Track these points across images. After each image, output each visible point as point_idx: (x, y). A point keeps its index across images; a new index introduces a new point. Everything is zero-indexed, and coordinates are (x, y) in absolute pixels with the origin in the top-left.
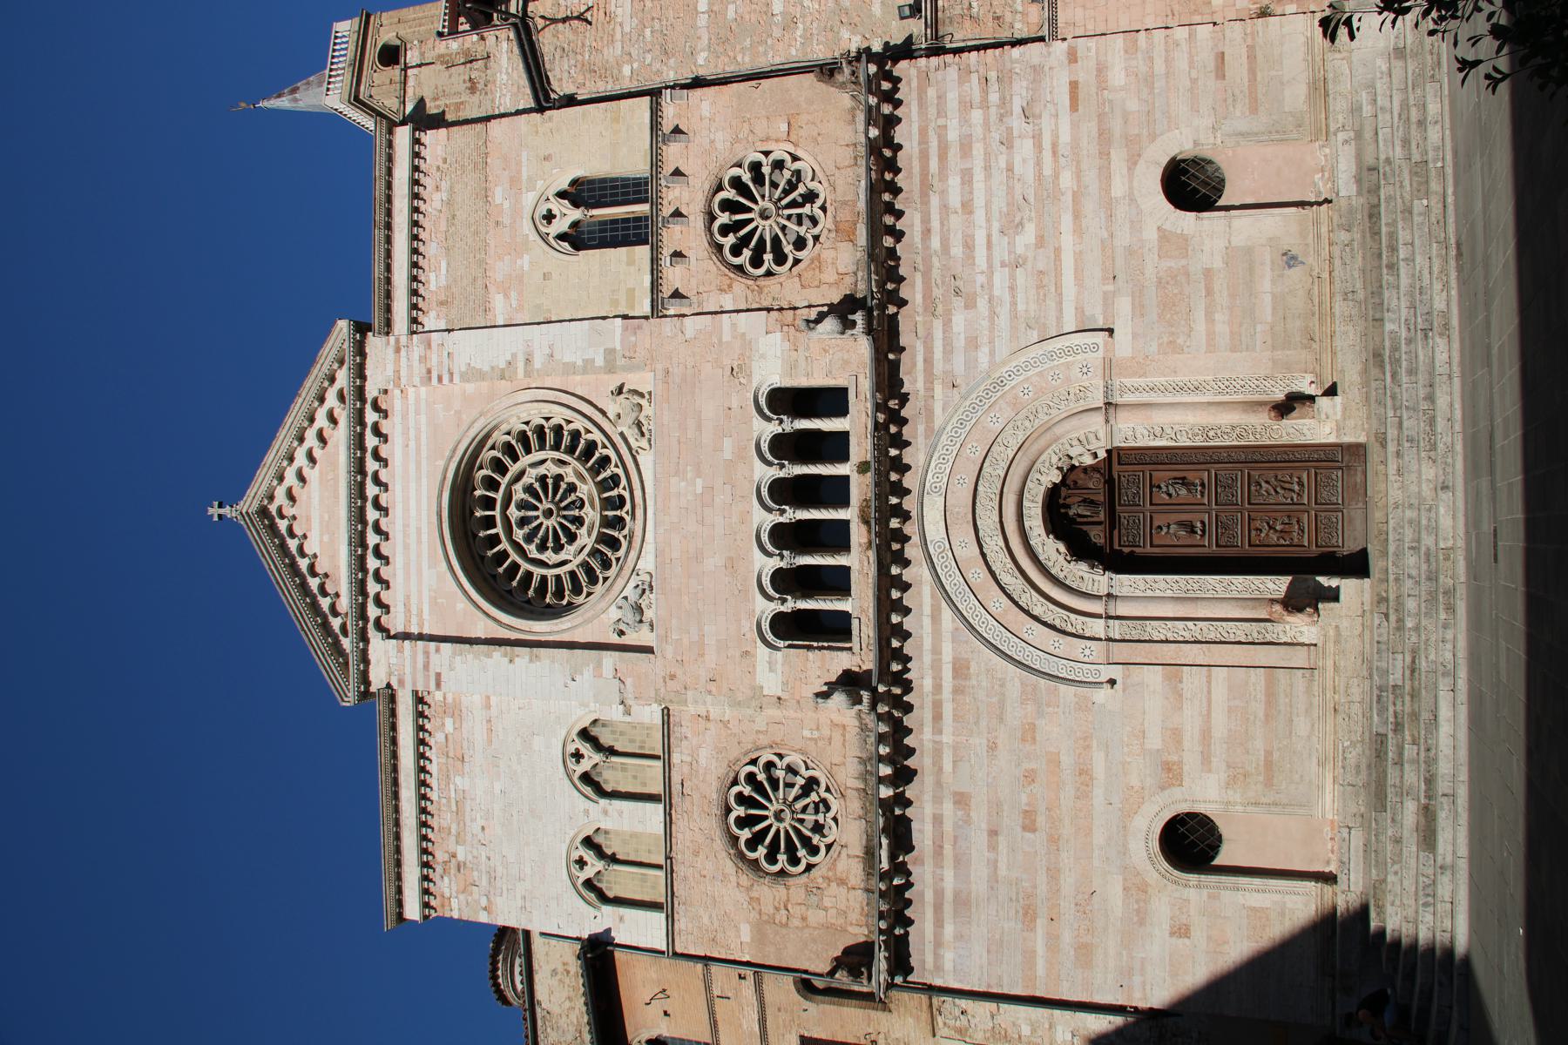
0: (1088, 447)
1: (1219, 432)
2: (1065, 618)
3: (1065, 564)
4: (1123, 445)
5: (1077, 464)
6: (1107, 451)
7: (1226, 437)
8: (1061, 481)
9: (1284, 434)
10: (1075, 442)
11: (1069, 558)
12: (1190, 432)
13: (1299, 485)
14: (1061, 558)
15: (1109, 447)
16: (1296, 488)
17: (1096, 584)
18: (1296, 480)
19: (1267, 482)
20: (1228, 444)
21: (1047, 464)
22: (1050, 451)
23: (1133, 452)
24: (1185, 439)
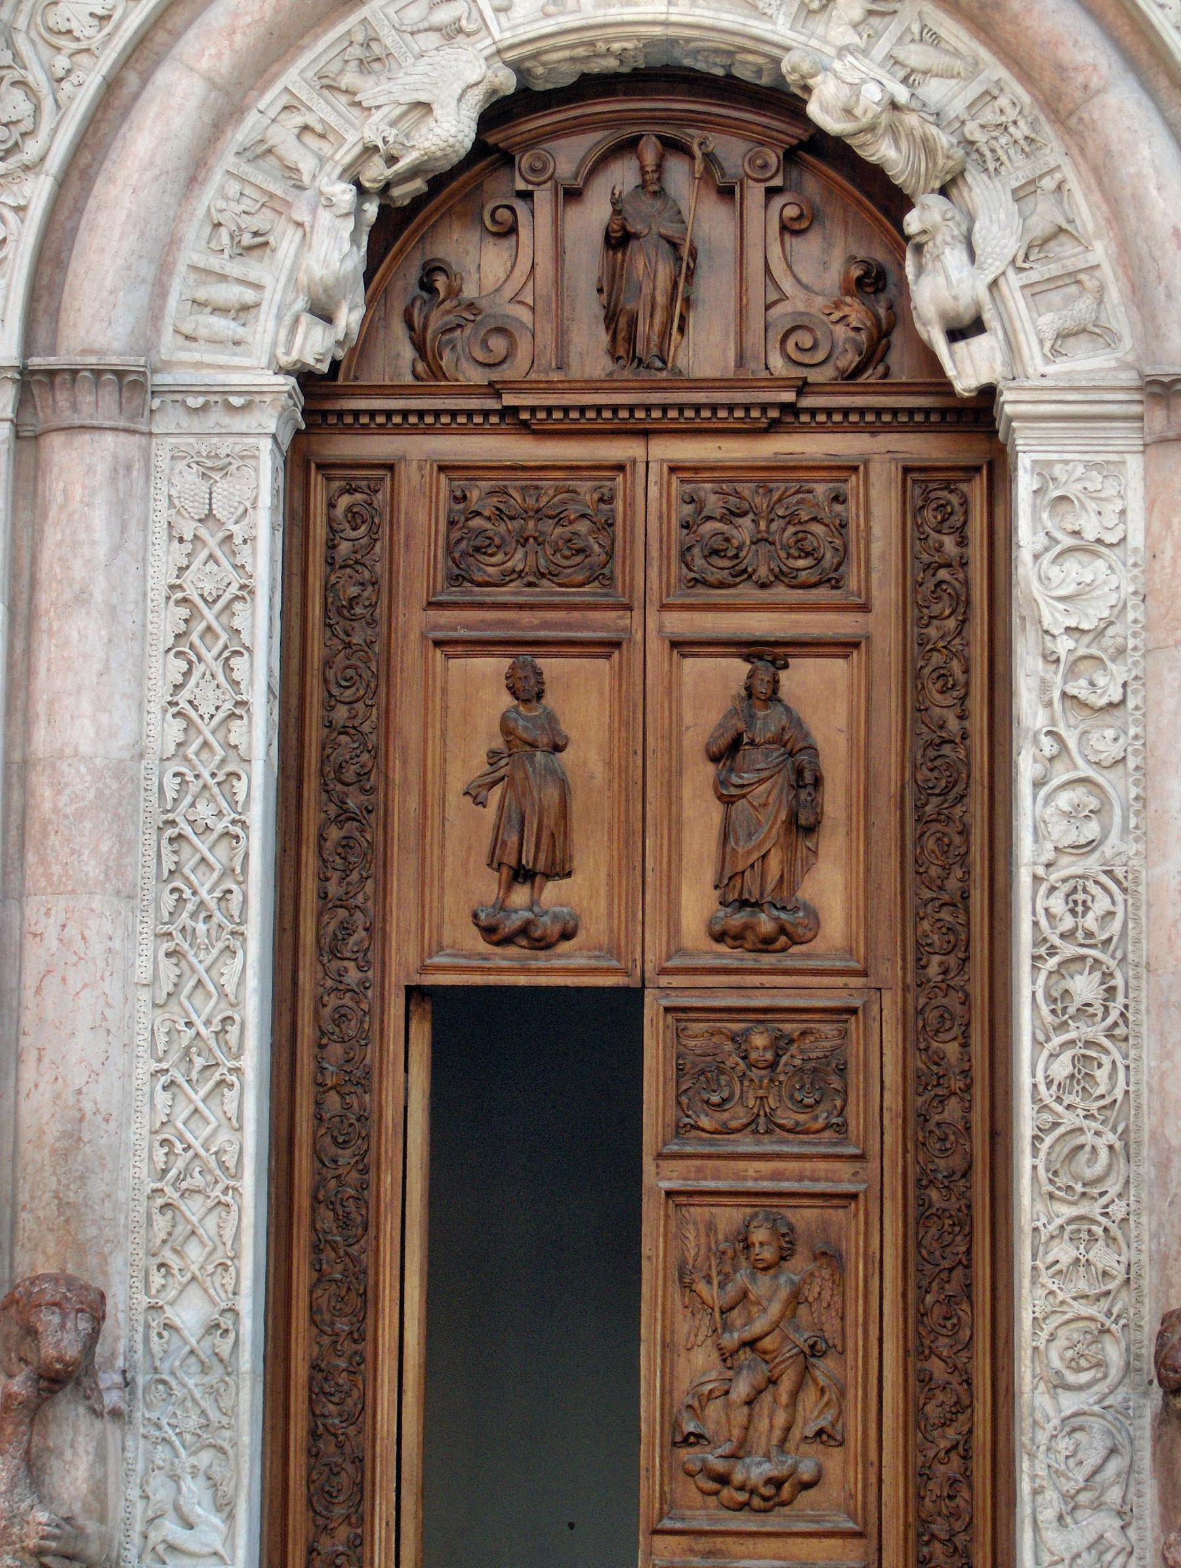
0: (1014, 280)
1: (1096, 1032)
2: (32, 149)
3: (345, 155)
4: (1025, 484)
5: (913, 222)
6: (988, 393)
7: (1062, 1068)
8: (820, 133)
9: (1070, 1403)
10: (1045, 214)
11: (375, 172)
12: (1091, 864)
13: (777, 1483)
14: (374, 130)
15: (1010, 403)
16: (757, 1470)
17: (222, 326)
18: (806, 1471)
19: (796, 1298)
20: (1024, 1079)
21: (916, 55)
22: (996, 71)
23: (977, 552)
24: (1062, 833)
